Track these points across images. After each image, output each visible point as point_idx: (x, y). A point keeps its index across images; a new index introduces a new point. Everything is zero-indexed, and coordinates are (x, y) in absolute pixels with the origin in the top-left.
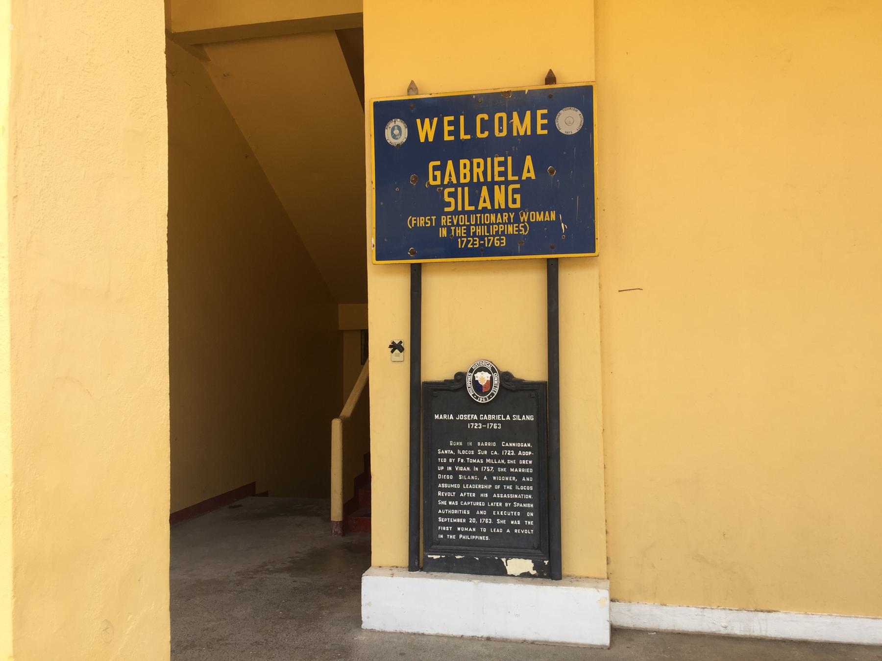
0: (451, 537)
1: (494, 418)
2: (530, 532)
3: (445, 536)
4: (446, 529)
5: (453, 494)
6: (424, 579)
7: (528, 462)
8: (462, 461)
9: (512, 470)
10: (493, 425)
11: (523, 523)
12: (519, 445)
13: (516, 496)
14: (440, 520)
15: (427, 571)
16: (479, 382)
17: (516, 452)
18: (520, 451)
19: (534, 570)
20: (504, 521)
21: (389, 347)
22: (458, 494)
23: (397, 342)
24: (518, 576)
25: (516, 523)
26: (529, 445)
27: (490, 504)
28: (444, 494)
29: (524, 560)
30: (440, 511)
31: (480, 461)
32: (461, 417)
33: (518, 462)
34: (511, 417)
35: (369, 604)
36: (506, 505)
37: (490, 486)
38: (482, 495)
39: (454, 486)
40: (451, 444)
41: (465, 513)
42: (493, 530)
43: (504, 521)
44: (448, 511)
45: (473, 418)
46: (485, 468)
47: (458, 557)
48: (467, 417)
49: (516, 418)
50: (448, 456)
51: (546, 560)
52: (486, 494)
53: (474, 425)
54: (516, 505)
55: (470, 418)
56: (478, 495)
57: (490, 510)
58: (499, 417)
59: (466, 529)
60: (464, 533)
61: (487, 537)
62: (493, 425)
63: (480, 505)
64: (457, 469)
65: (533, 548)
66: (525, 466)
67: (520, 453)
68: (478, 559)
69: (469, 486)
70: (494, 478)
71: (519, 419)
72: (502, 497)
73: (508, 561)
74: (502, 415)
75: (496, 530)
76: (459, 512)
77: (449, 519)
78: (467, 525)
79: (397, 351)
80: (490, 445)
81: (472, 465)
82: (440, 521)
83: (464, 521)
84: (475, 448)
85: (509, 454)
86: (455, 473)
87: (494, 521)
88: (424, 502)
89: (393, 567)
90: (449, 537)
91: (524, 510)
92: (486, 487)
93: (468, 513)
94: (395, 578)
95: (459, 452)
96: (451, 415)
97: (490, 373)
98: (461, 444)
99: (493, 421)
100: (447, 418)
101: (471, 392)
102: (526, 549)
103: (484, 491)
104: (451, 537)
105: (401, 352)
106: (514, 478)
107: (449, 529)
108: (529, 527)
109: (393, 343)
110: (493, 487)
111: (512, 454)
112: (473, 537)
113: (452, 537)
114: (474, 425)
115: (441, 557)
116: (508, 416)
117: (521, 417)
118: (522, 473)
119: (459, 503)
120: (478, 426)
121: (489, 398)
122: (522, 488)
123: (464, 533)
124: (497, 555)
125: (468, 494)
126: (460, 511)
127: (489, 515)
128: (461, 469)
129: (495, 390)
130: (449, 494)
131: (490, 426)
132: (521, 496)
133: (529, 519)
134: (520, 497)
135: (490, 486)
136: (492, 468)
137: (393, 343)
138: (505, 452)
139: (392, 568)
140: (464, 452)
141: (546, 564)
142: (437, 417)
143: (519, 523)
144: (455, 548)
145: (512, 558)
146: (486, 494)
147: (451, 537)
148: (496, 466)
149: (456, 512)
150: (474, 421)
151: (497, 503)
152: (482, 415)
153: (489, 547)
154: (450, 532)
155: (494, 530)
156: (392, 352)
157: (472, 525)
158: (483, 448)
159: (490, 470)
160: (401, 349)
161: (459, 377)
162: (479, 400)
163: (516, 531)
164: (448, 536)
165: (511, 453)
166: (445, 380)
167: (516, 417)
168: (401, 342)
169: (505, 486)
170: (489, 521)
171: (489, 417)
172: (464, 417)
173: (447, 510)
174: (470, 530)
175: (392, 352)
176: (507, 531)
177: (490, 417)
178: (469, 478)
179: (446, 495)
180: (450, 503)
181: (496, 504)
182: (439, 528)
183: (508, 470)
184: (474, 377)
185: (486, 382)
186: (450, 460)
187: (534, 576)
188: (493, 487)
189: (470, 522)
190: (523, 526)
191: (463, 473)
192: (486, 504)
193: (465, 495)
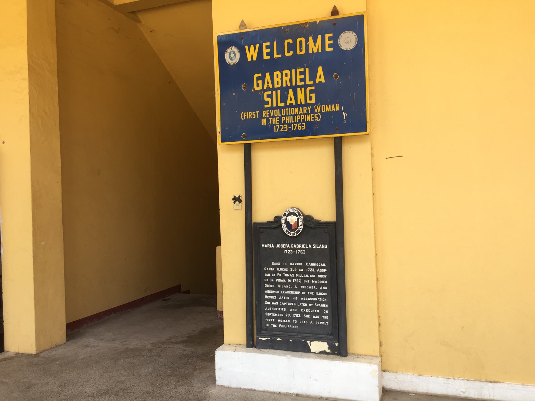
0: (274, 326)
1: (300, 246)
2: (326, 323)
3: (270, 325)
4: (270, 320)
5: (274, 297)
6: (255, 353)
7: (324, 276)
8: (280, 275)
9: (313, 282)
10: (300, 251)
11: (321, 317)
12: (317, 265)
13: (316, 299)
14: (267, 314)
15: (259, 348)
16: (290, 222)
17: (316, 269)
18: (318, 269)
19: (328, 349)
20: (309, 316)
21: (232, 200)
22: (278, 298)
23: (237, 196)
24: (318, 353)
25: (316, 317)
26: (324, 265)
27: (299, 304)
28: (269, 297)
30: (266, 309)
31: (292, 275)
32: (279, 246)
33: (317, 276)
34: (312, 246)
35: (220, 369)
37: (299, 292)
38: (293, 298)
39: (275, 292)
40: (273, 264)
41: (283, 310)
42: (301, 322)
43: (309, 316)
44: (271, 309)
45: (287, 247)
46: (296, 280)
47: (278, 339)
48: (282, 246)
49: (316, 246)
50: (271, 272)
51: (337, 343)
52: (297, 298)
53: (288, 252)
54: (316, 305)
55: (285, 246)
56: (291, 298)
57: (299, 308)
58: (304, 246)
59: (284, 321)
60: (283, 323)
61: (297, 326)
62: (300, 251)
63: (293, 305)
64: (277, 281)
65: (328, 334)
66: (322, 279)
67: (318, 270)
68: (291, 341)
69: (285, 292)
70: (302, 287)
71: (317, 247)
72: (307, 300)
73: (311, 343)
74: (306, 245)
75: (303, 322)
76: (279, 309)
77: (272, 314)
78: (284, 318)
79: (237, 202)
81: (286, 278)
83: (282, 315)
84: (289, 267)
85: (311, 271)
86: (276, 284)
87: (302, 316)
88: (256, 302)
89: (237, 344)
90: (273, 326)
91: (321, 309)
92: (296, 293)
93: (285, 310)
94: (236, 352)
95: (278, 269)
96: (273, 245)
97: (297, 216)
98: (279, 264)
100: (270, 246)
101: (285, 229)
102: (323, 335)
103: (295, 295)
104: (274, 326)
105: (240, 203)
106: (315, 287)
107: (273, 320)
108: (325, 320)
109: (235, 197)
110: (301, 293)
112: (288, 326)
113: (275, 326)
114: (288, 252)
116: (310, 245)
117: (318, 246)
118: (320, 284)
119: (279, 303)
120: (290, 252)
122: (320, 294)
123: (283, 323)
124: (304, 339)
125: (285, 297)
126: (280, 308)
127: (298, 312)
128: (280, 280)
129: (301, 228)
130: (272, 297)
131: (298, 252)
132: (320, 299)
133: (325, 315)
135: (299, 292)
136: (300, 280)
137: (235, 197)
138: (308, 270)
139: (237, 345)
140: (281, 269)
141: (337, 345)
142: (263, 246)
143: (318, 318)
145: (314, 341)
146: (297, 298)
147: (273, 326)
148: (302, 279)
149: (277, 309)
150: (288, 249)
151: (304, 304)
152: (293, 245)
153: (299, 333)
154: (273, 323)
156: (234, 203)
157: (287, 318)
158: (294, 267)
159: (299, 281)
160: (240, 201)
162: (290, 235)
163: (316, 323)
164: (272, 325)
165: (312, 270)
166: (268, 221)
167: (315, 246)
168: (240, 196)
169: (309, 292)
170: (298, 316)
171: (297, 246)
172: (281, 246)
173: (271, 308)
174: (286, 321)
175: (234, 203)
176: (311, 323)
177: (298, 246)
178: (285, 286)
179: (270, 298)
180: (273, 303)
181: (303, 304)
182: (266, 320)
183: (310, 281)
184: (286, 219)
185: (294, 222)
186: (273, 275)
187: (328, 354)
188: (301, 293)
189: (286, 316)
190: (321, 320)
191: (281, 283)
192: (297, 304)
193: (282, 298)
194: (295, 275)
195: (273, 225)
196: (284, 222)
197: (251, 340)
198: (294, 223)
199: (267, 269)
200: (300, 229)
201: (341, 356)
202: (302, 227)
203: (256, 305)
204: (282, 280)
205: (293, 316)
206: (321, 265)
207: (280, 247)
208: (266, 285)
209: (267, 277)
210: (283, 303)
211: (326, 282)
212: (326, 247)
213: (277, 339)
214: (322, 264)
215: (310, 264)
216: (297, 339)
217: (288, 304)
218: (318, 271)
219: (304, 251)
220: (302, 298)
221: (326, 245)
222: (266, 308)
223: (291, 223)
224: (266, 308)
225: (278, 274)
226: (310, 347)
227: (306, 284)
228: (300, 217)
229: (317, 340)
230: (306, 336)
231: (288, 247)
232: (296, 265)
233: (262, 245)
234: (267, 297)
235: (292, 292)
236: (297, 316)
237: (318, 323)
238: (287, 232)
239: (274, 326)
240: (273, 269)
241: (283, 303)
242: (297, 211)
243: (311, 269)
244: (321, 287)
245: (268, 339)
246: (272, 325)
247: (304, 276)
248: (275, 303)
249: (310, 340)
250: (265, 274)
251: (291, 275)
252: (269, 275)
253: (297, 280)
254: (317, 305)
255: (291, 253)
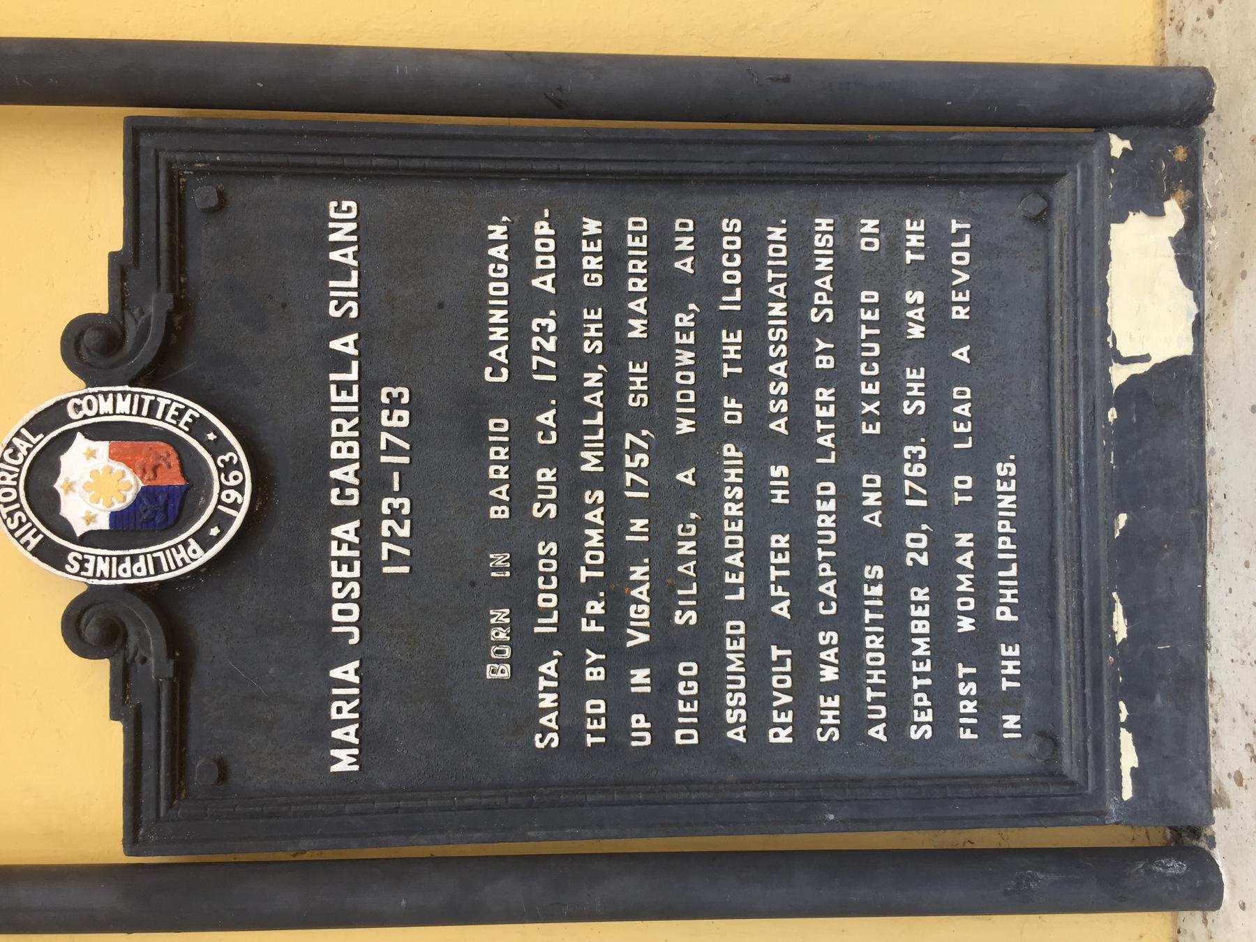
0: (1010, 668)
1: (346, 425)
2: (960, 235)
3: (1011, 702)
4: (968, 697)
5: (781, 661)
7: (592, 238)
9: (638, 328)
10: (390, 430)
12: (498, 289)
13: (778, 309)
14: (920, 731)
15: (1209, 800)
16: (118, 506)
17: (539, 302)
18: (536, 283)
19: (1161, 213)
20: (911, 374)
22: (781, 632)
24: (1198, 299)
26: (498, 232)
27: (825, 452)
28: (783, 709)
29: (1113, 265)
31: (595, 505)
34: (342, 327)
36: (824, 362)
37: (729, 450)
39: (735, 651)
40: (504, 672)
42: (962, 437)
43: (911, 374)
44: (875, 688)
45: (351, 546)
46: (629, 476)
51: (1108, 147)
52: (775, 472)
53: (393, 538)
54: (821, 310)
55: (349, 562)
58: (344, 397)
60: (986, 593)
61: (1001, 469)
62: (390, 430)
63: (832, 506)
64: (643, 638)
65: (1041, 220)
66: (615, 259)
67: (545, 284)
68: (1123, 519)
69: (733, 569)
70: (685, 427)
71: (354, 283)
72: (784, 387)
73: (1125, 353)
74: (333, 377)
75: (961, 419)
76: (873, 622)
80: (503, 451)
82: (928, 732)
85: (550, 346)
88: (832, 827)
92: (733, 476)
93: (878, 571)
95: (546, 626)
96: (336, 673)
97: (65, 441)
99: (368, 431)
100: (348, 699)
102: (1048, 261)
103: (755, 484)
104: (1010, 668)
106: (683, 320)
107: (967, 678)
108: (937, 243)
110: (732, 434)
111: (552, 327)
112: (1004, 543)
115: (1129, 725)
116: (335, 345)
117: (342, 271)
118: (652, 277)
119: (827, 623)
120: (395, 514)
121: (219, 447)
123: (986, 593)
124: (1094, 414)
125: (774, 573)
126: (868, 616)
128: (640, 613)
130: (781, 679)
131: (392, 449)
132: (776, 281)
133: (893, 241)
134: (779, 290)
135: (729, 450)
136: (629, 437)
138: (542, 369)
140: (547, 600)
141: (1127, 144)
143: (919, 296)
144: (1066, 646)
145: (1106, 330)
146: (775, 472)
147: (1010, 671)
148: (617, 420)
149: (874, 642)
150: (369, 539)
151: (821, 412)
152: (335, 492)
153: (1050, 456)
154: (987, 677)
155: (962, 429)
157: (942, 551)
158: (523, 491)
159: (642, 450)
161: (91, 631)
162: (235, 506)
163: (959, 313)
164: (1005, 684)
165: (543, 332)
166: (114, 716)
167: (341, 302)
169: (726, 370)
170: (914, 459)
171: (344, 455)
172: (347, 599)
173: (870, 695)
174: (966, 560)
176: (965, 359)
179: (787, 699)
180: (829, 674)
181: (825, 420)
182: (967, 735)
183: (638, 350)
184: (91, 539)
185: (119, 467)
186: (595, 675)
187: (1194, 215)
188: (732, 434)
189: (924, 560)
191: (663, 603)
192: (825, 473)
193: (780, 593)
194: (592, 481)
195: (152, 661)
196: (121, 559)
197: (1150, 872)
198: (130, 465)
199: (543, 721)
200: (186, 418)
201: (1210, 109)
202: (163, 403)
203: (859, 824)
204: (635, 593)
205: (923, 503)
206: (498, 261)
207: (355, 608)
208: (679, 733)
209: (618, 727)
210: (822, 589)
211: (637, 223)
212: (345, 204)
213: (1119, 639)
214: (493, 252)
215: (493, 354)
216: (1100, 473)
217: (825, 548)
218: (549, 288)
219: (385, 400)
220: (773, 426)
221: (333, 204)
222: (872, 732)
223: (130, 497)
224: (872, 732)
225: (584, 628)
226: (1157, 358)
227: (661, 385)
228: (72, 413)
229: (1097, 307)
230: (1069, 388)
231: (357, 532)
232: (503, 469)
233: (335, 768)
234: (784, 726)
235: (732, 509)
236: (920, 470)
237: (960, 298)
238: (214, 531)
239: (1010, 664)
240: (543, 669)
241: (822, 589)
242: (17, 442)
243: (535, 339)
244: (678, 265)
245: (1124, 715)
246: (1005, 684)
247: (598, 403)
248: (823, 655)
249: (1098, 362)
250: (590, 740)
251: (589, 516)
252: (595, 706)
253: (628, 464)
254: (820, 308)
255: (406, 511)
